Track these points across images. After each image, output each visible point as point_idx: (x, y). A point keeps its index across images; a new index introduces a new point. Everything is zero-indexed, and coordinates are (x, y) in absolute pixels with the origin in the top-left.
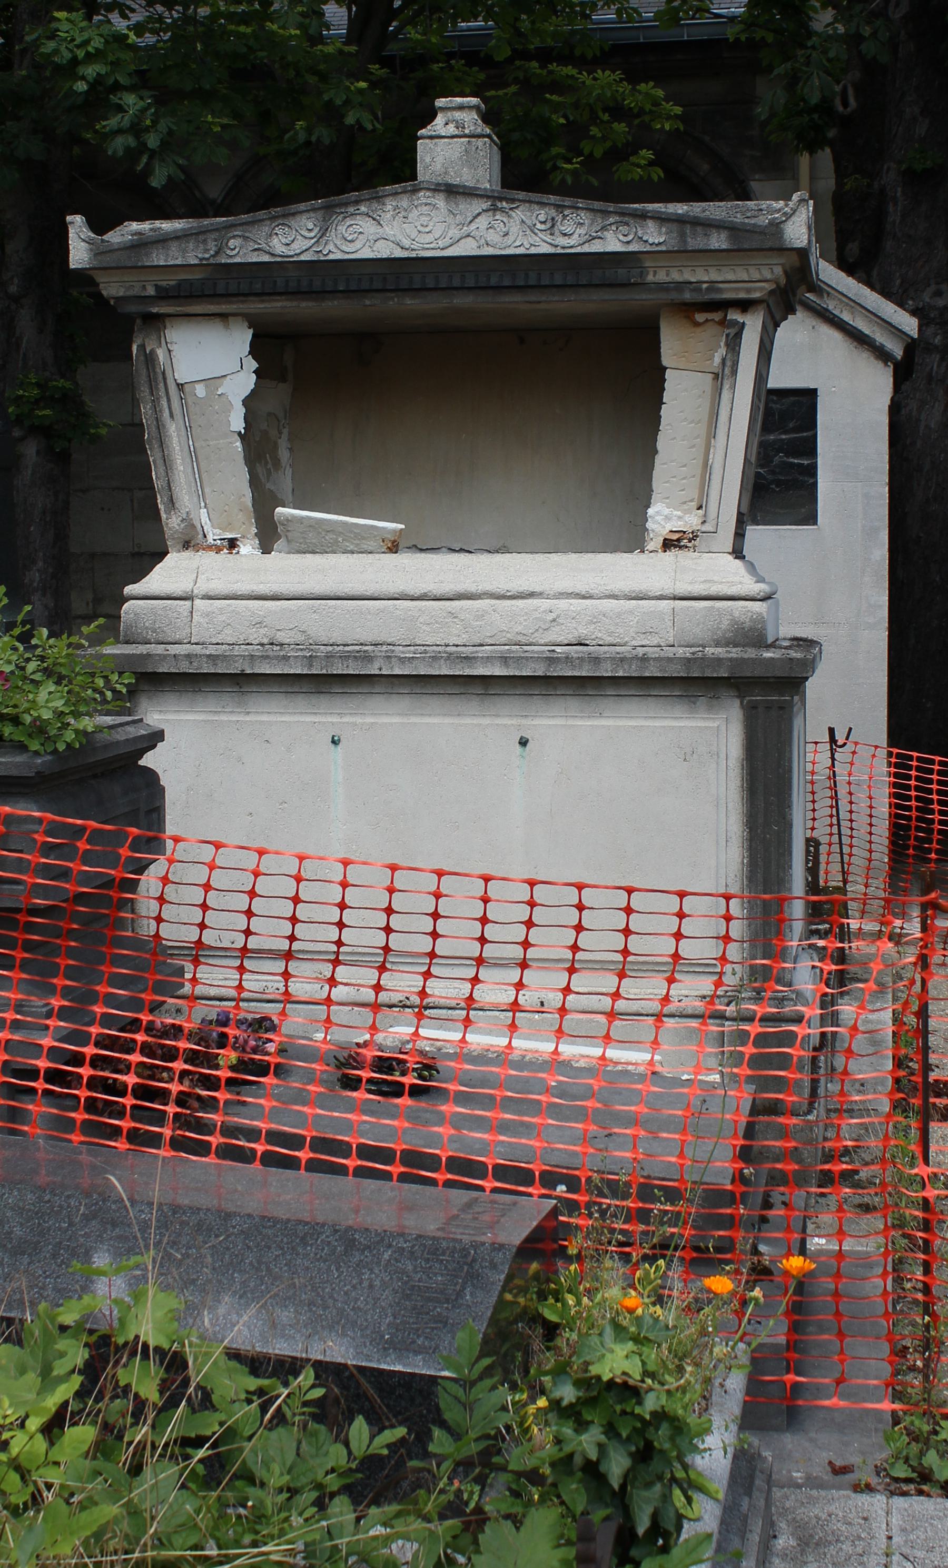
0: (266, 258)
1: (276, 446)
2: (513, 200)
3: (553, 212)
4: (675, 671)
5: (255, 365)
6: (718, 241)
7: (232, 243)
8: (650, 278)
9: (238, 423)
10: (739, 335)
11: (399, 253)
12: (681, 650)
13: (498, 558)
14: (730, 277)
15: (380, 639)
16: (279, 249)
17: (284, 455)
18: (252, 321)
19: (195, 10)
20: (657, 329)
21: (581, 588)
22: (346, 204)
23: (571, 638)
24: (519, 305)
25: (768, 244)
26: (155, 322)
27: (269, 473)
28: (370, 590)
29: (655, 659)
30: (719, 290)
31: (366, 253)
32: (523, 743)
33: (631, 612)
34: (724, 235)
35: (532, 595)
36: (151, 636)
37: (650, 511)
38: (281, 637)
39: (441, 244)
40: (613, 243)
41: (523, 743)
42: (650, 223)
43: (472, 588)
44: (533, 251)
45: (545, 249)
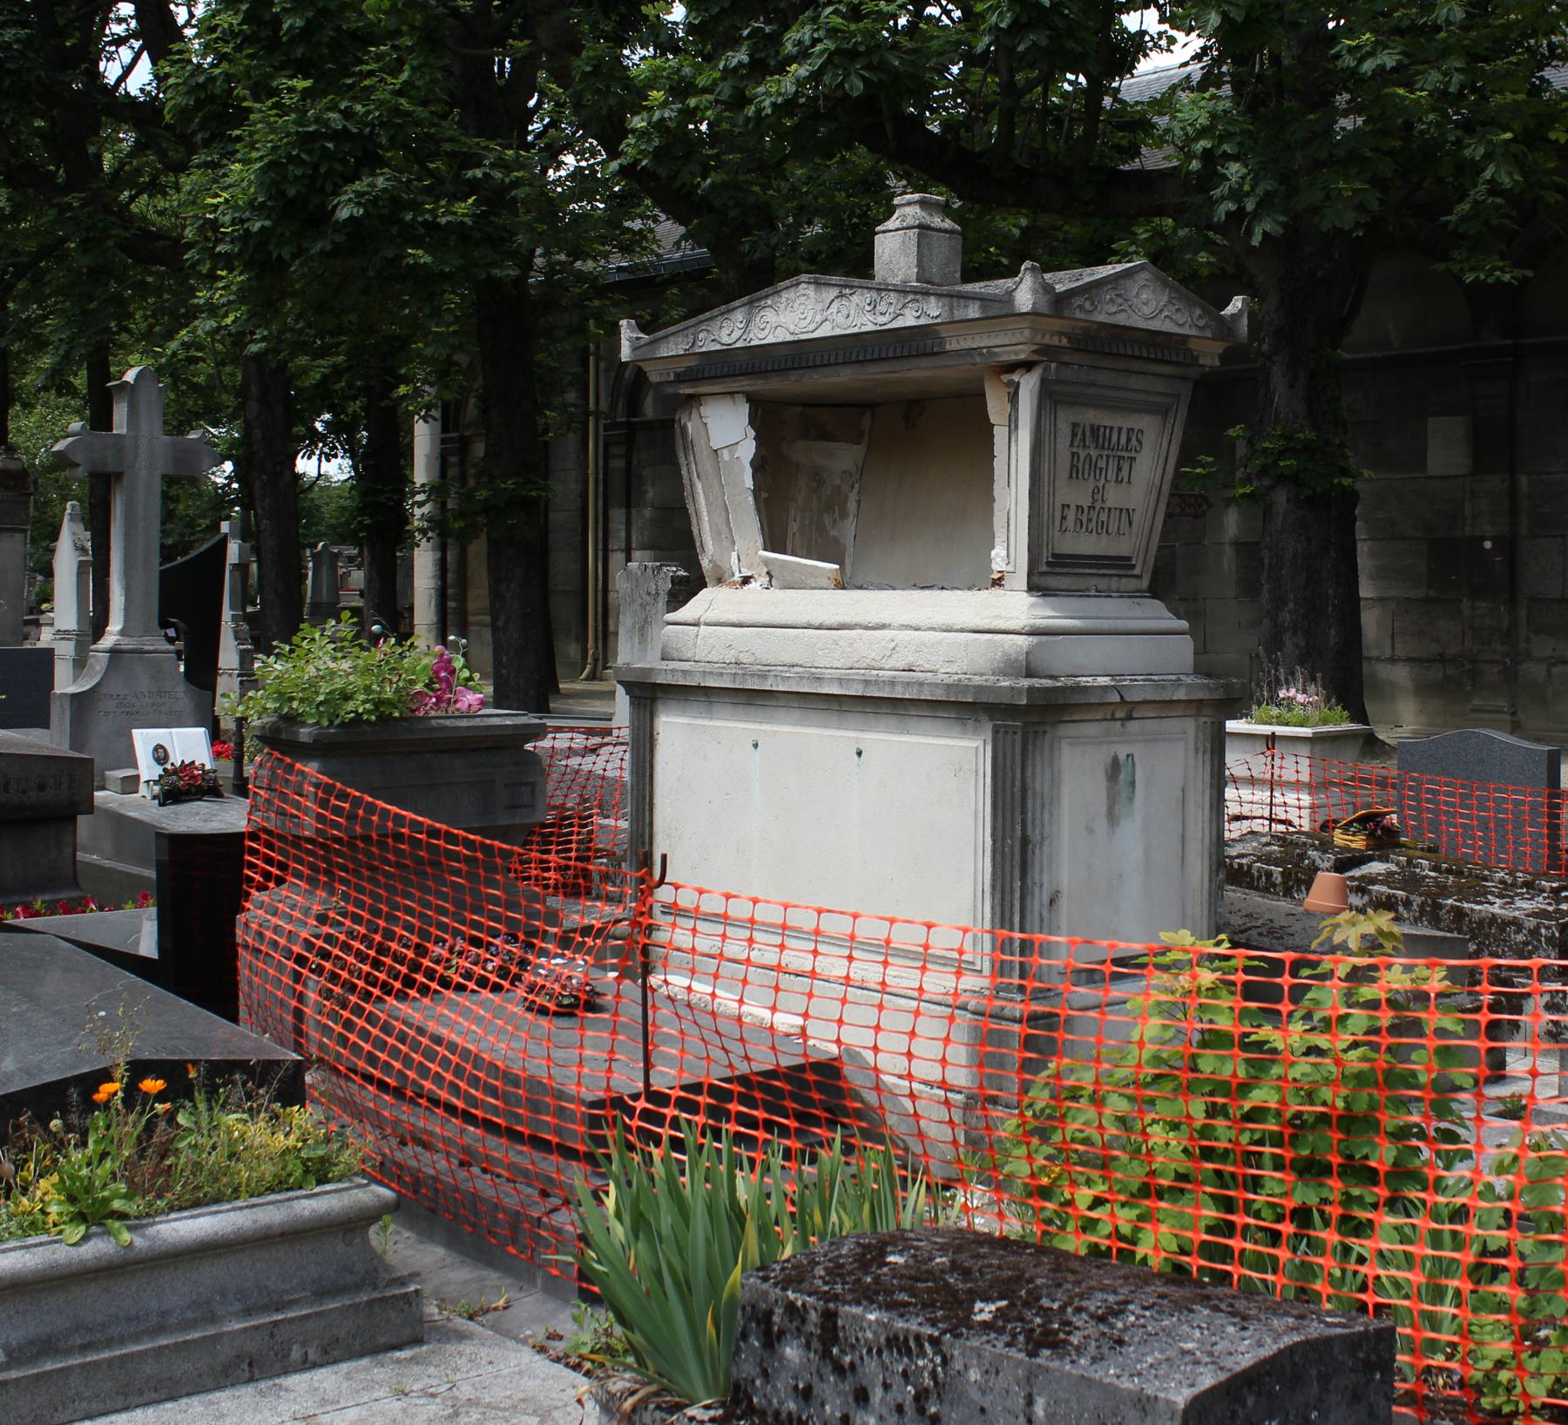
0: (718, 347)
1: (846, 498)
2: (851, 287)
3: (875, 294)
4: (940, 695)
5: (753, 433)
6: (973, 311)
7: (701, 336)
8: (948, 347)
9: (749, 483)
10: (1016, 393)
11: (790, 338)
12: (977, 678)
13: (927, 592)
14: (998, 342)
15: (795, 661)
16: (726, 340)
17: (852, 505)
18: (752, 399)
19: (132, 199)
20: (984, 395)
21: (914, 623)
22: (760, 299)
23: (900, 665)
24: (843, 378)
25: (1005, 311)
26: (693, 401)
27: (835, 521)
28: (784, 620)
29: (930, 684)
30: (996, 354)
31: (771, 340)
32: (859, 754)
33: (940, 643)
34: (977, 304)
35: (883, 627)
36: (676, 655)
37: (993, 553)
38: (744, 658)
39: (811, 328)
40: (909, 319)
41: (859, 754)
42: (932, 299)
43: (849, 620)
44: (864, 329)
45: (870, 328)
